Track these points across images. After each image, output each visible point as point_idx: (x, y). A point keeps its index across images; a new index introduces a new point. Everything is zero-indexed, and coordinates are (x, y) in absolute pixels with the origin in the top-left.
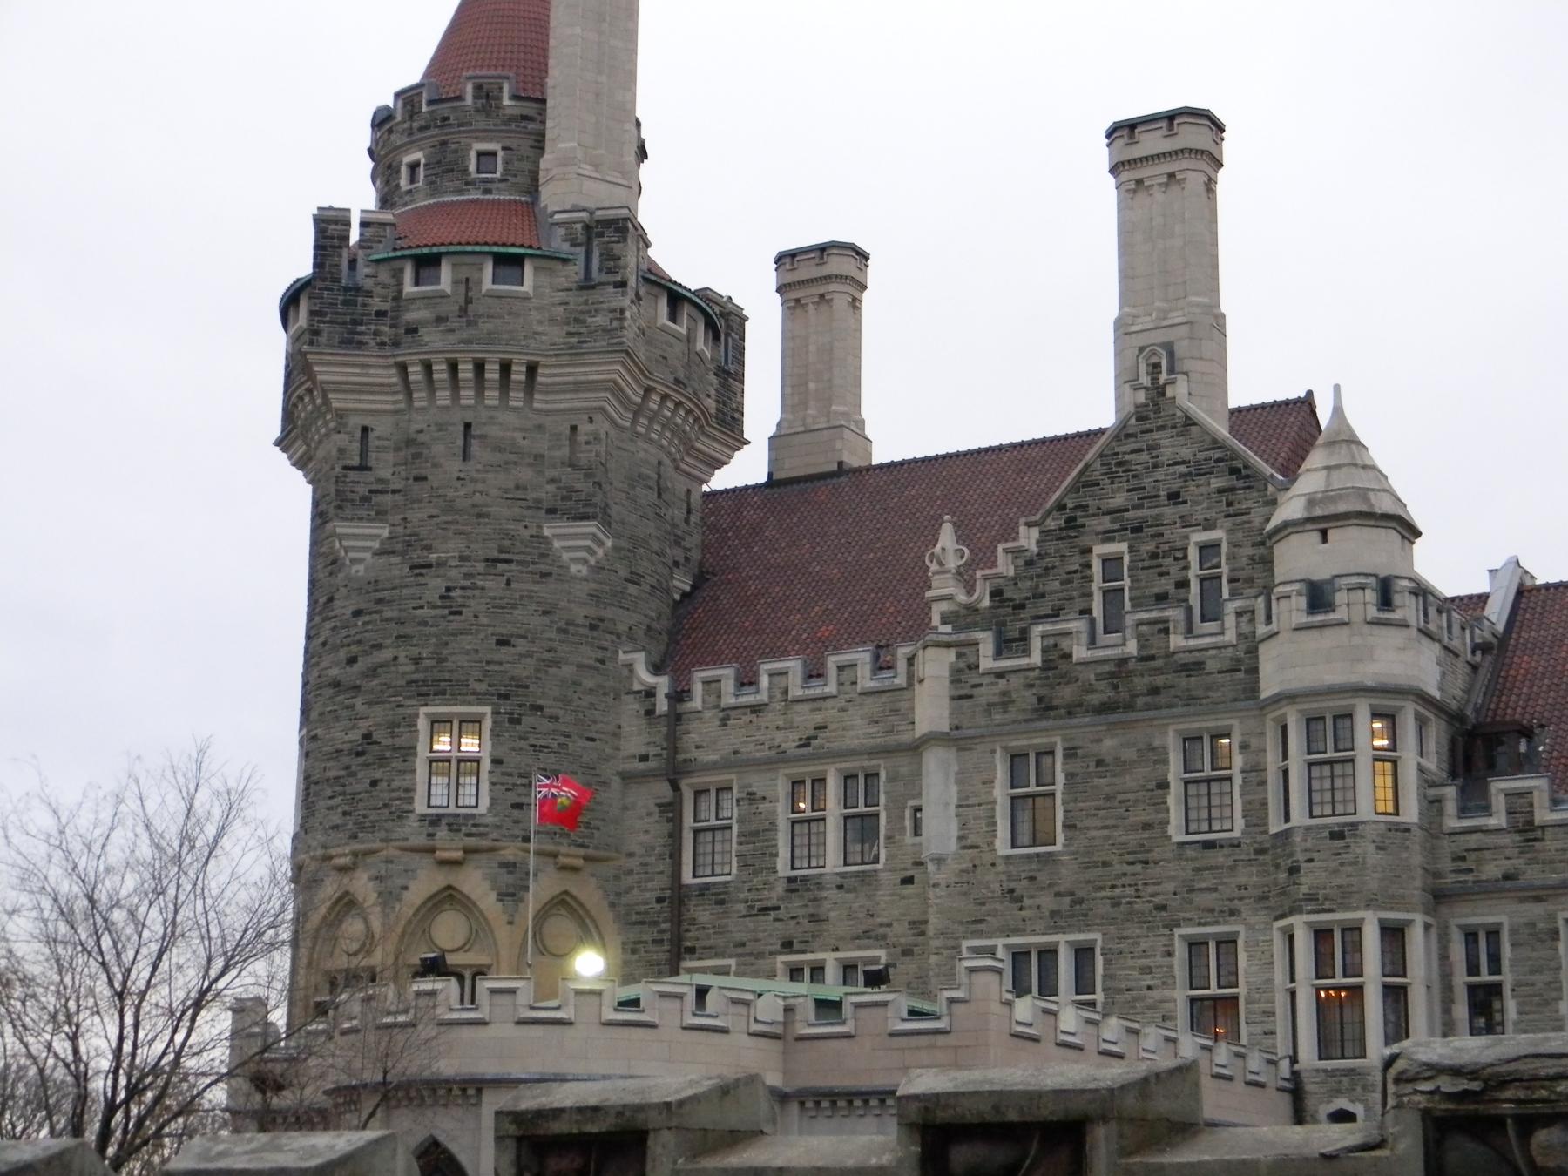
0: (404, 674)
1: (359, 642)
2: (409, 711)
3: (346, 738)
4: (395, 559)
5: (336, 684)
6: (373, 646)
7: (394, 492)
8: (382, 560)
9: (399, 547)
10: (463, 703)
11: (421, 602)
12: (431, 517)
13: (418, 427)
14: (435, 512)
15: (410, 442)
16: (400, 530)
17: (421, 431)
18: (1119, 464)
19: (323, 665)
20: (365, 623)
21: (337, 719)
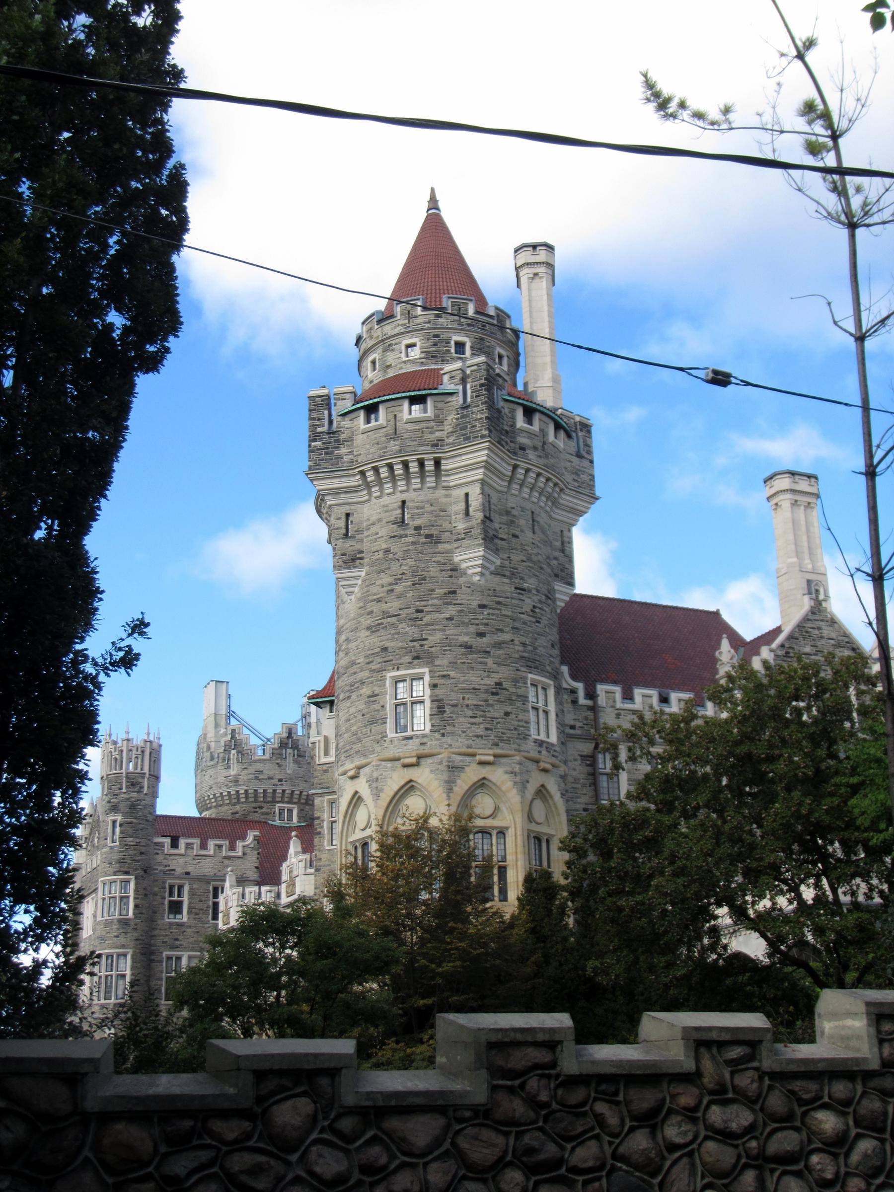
0: (518, 651)
1: (487, 625)
2: (524, 674)
3: (482, 682)
4: (507, 581)
5: (468, 647)
6: (497, 630)
7: (502, 539)
8: (497, 579)
9: (507, 573)
10: (546, 677)
11: (523, 610)
12: (523, 561)
13: (513, 505)
14: (524, 559)
15: (508, 513)
16: (507, 563)
17: (513, 508)
18: (807, 632)
19: (448, 632)
20: (489, 614)
21: (472, 668)
